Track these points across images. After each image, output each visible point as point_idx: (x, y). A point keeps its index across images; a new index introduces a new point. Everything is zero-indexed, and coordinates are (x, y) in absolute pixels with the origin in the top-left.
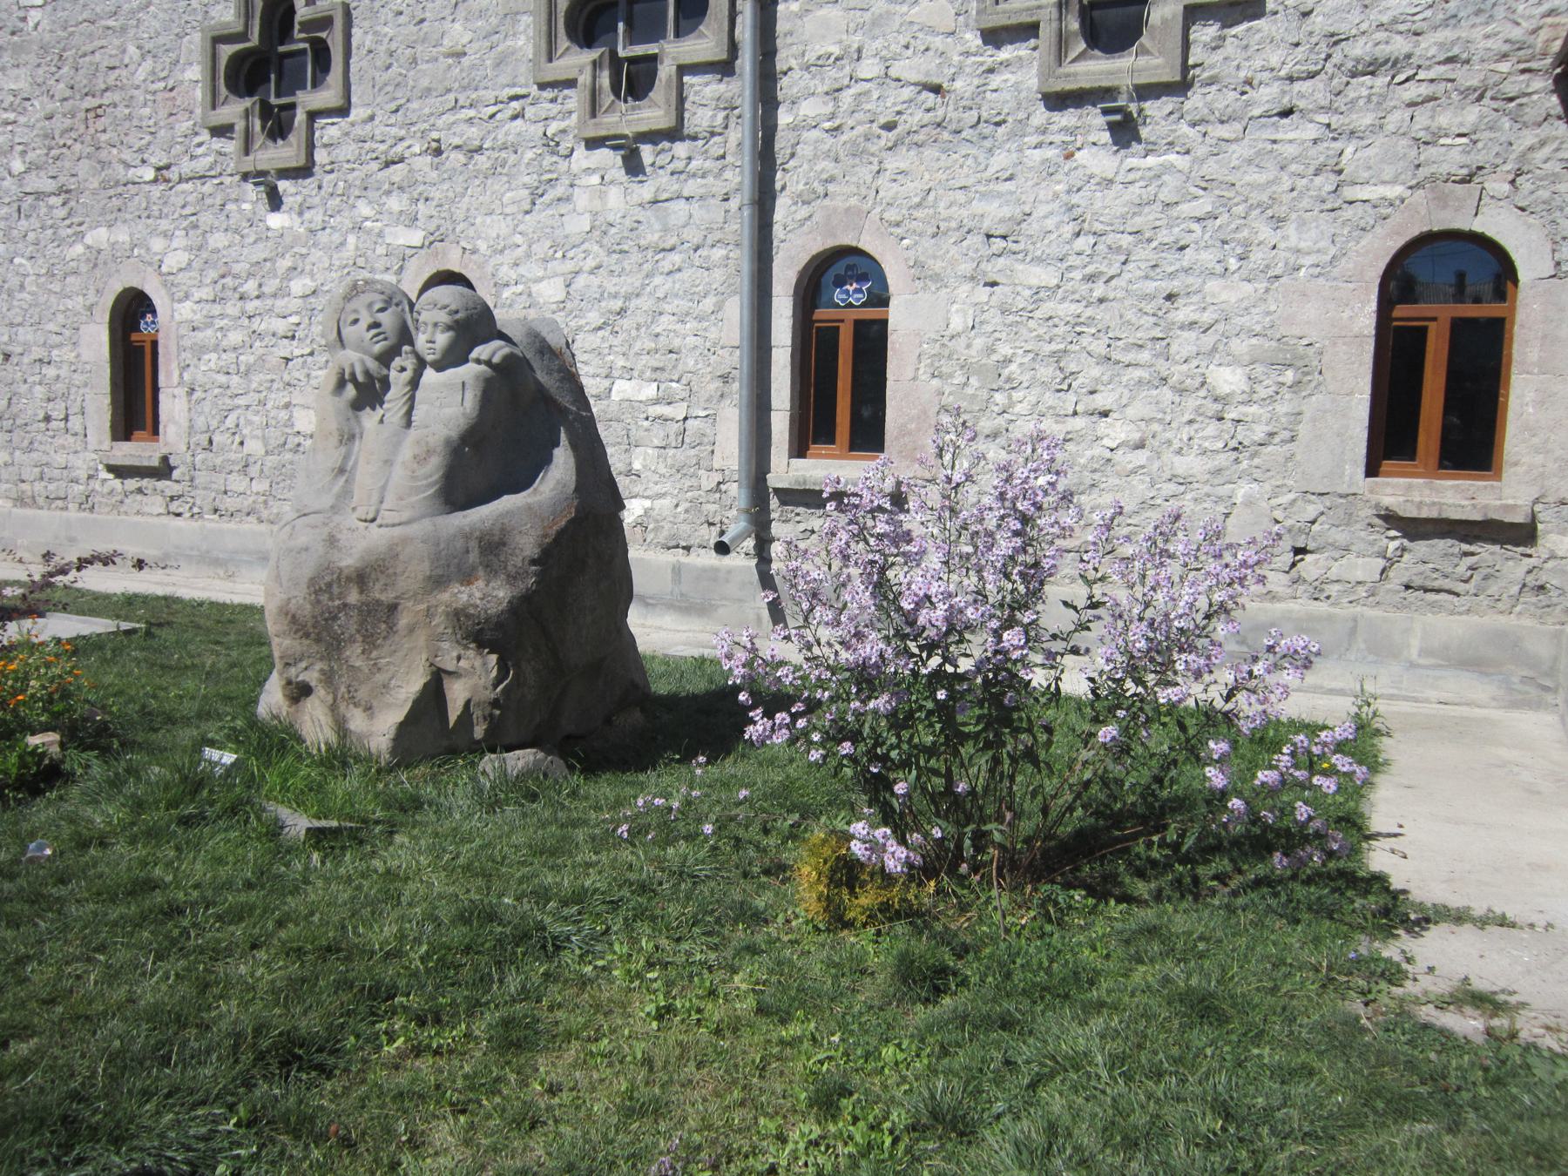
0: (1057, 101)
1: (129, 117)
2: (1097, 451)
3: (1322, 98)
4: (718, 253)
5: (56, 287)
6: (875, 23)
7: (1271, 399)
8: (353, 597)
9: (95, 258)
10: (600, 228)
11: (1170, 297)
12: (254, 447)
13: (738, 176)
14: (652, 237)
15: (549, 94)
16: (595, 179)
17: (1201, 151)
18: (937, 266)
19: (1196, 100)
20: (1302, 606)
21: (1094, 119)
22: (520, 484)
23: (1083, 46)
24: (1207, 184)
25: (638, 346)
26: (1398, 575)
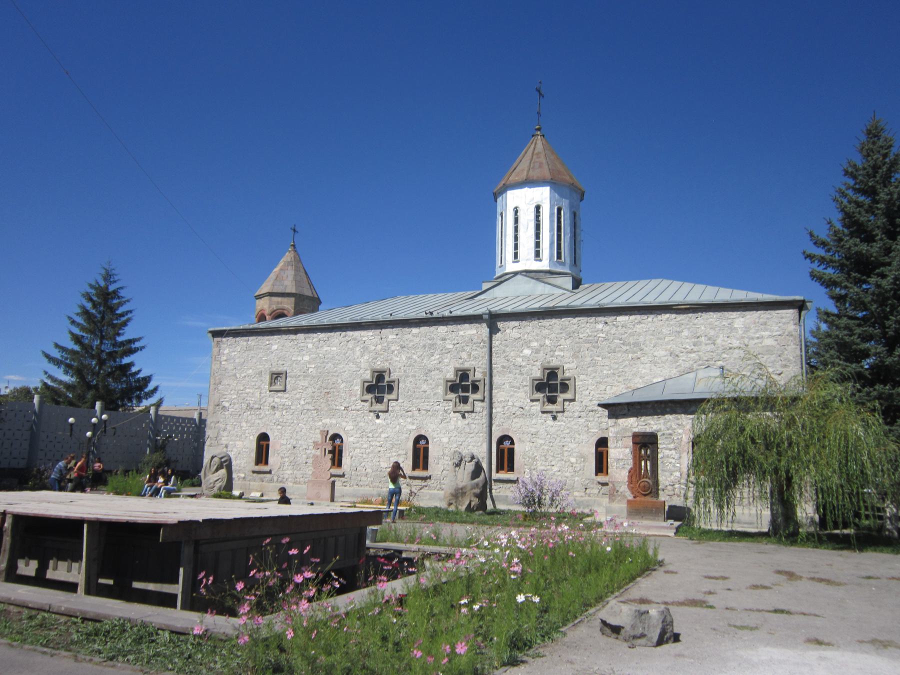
0: (543, 412)
1: (338, 395)
2: (552, 472)
3: (585, 415)
4: (481, 435)
5: (313, 432)
6: (511, 396)
7: (580, 463)
8: (460, 491)
10: (457, 428)
11: (563, 446)
12: (369, 470)
13: (485, 420)
14: (468, 430)
15: (445, 402)
16: (456, 419)
17: (567, 422)
19: (565, 414)
20: (587, 498)
21: (549, 415)
22: (478, 477)
23: (547, 403)
24: (568, 428)
26: (601, 492)
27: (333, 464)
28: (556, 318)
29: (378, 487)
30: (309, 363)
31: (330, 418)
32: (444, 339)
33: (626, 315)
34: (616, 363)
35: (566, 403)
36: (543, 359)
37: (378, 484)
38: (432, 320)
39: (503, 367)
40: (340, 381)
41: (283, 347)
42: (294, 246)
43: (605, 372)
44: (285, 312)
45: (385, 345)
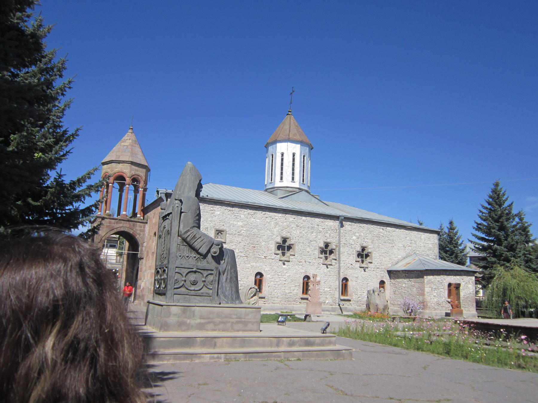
0: (360, 267)
4: (335, 277)
9: (252, 267)
12: (279, 294)
13: (336, 270)
18: (352, 280)
21: (363, 269)
25: (327, 285)
27: (303, 293)
28: (365, 224)
29: (284, 304)
30: (242, 227)
31: (256, 263)
32: (318, 225)
33: (390, 227)
34: (386, 248)
35: (369, 264)
36: (360, 242)
37: (284, 302)
38: (314, 214)
39: (344, 244)
40: (261, 240)
41: (223, 213)
42: (132, 129)
43: (383, 251)
44: (125, 176)
45: (288, 223)
